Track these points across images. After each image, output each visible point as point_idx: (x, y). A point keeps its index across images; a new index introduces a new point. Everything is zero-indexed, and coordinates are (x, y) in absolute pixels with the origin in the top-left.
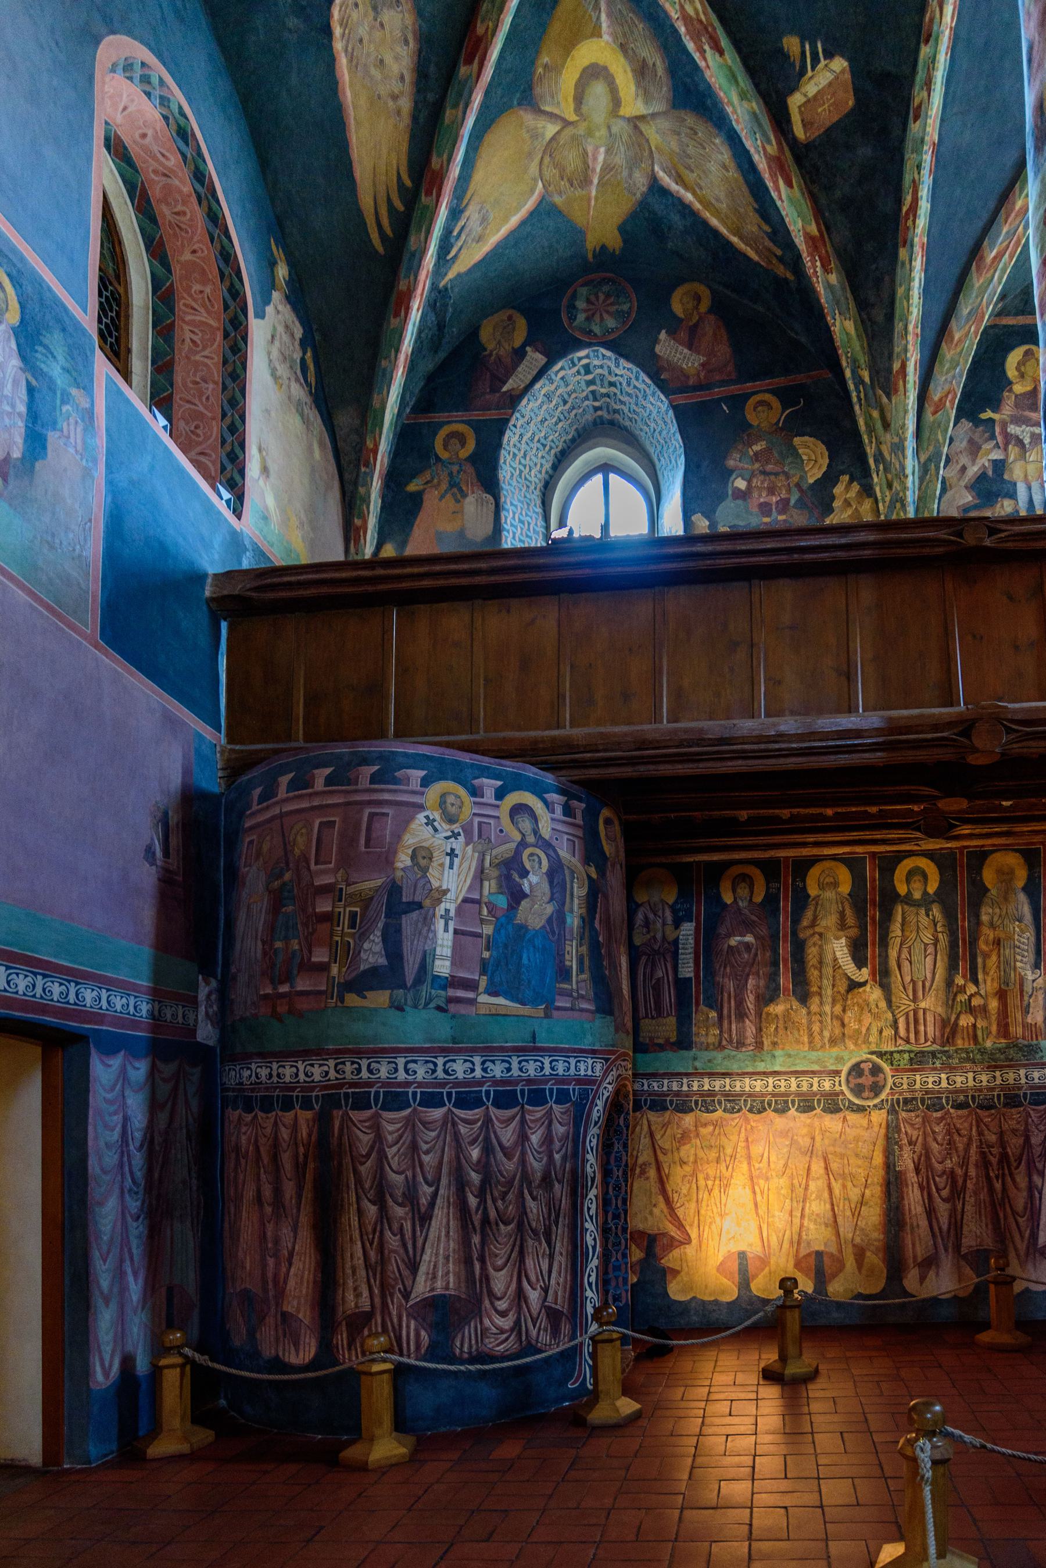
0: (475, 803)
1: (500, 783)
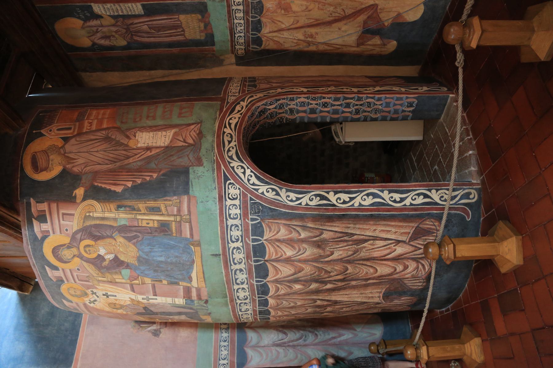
1: (47, 268)
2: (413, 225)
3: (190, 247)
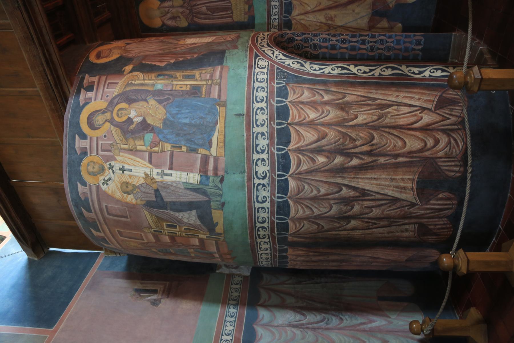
0: (91, 154)
1: (77, 136)
2: (436, 93)
3: (216, 107)
